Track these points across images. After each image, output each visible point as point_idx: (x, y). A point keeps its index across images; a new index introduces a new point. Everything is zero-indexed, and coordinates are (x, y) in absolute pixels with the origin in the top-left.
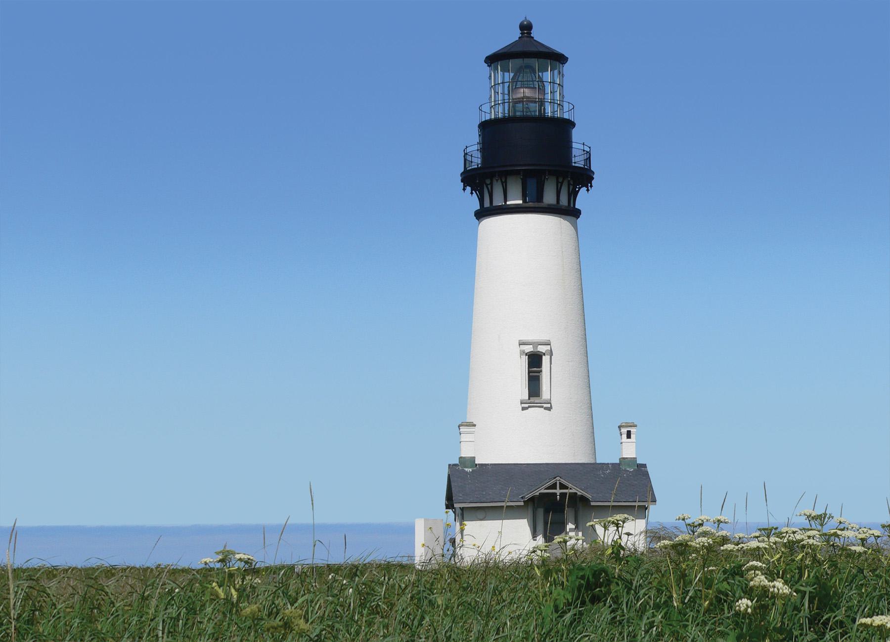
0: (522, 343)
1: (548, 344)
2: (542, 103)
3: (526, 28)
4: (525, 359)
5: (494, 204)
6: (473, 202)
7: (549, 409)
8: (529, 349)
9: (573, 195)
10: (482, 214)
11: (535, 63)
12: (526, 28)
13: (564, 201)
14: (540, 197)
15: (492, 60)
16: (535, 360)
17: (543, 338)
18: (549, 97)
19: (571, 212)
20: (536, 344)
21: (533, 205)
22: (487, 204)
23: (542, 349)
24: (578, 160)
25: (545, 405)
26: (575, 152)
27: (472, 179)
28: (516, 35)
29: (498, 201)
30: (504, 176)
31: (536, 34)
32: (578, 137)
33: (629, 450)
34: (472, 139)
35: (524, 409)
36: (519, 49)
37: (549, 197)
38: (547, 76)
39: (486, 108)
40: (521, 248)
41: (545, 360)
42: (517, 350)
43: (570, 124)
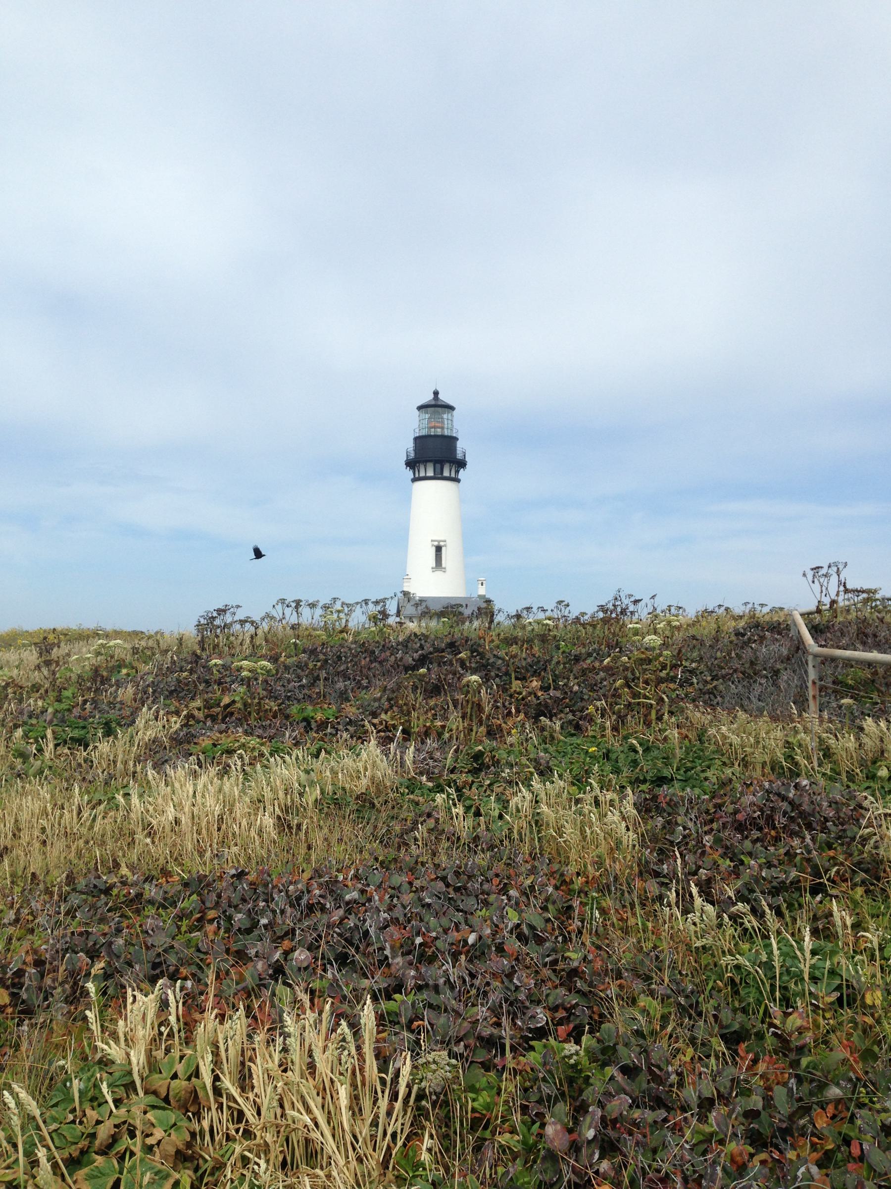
2: (443, 428)
3: (436, 393)
4: (434, 548)
6: (409, 474)
8: (436, 543)
9: (457, 472)
10: (414, 480)
11: (440, 409)
12: (436, 393)
14: (442, 473)
16: (439, 549)
17: (443, 539)
18: (446, 426)
20: (439, 541)
21: (438, 476)
22: (417, 475)
23: (442, 544)
24: (459, 456)
26: (458, 452)
27: (411, 464)
28: (432, 396)
29: (422, 474)
30: (425, 462)
31: (440, 396)
32: (460, 445)
33: (482, 591)
34: (410, 445)
36: (433, 403)
37: (446, 473)
38: (445, 416)
39: (417, 431)
40: (433, 497)
41: (443, 549)
42: (430, 544)
43: (456, 439)
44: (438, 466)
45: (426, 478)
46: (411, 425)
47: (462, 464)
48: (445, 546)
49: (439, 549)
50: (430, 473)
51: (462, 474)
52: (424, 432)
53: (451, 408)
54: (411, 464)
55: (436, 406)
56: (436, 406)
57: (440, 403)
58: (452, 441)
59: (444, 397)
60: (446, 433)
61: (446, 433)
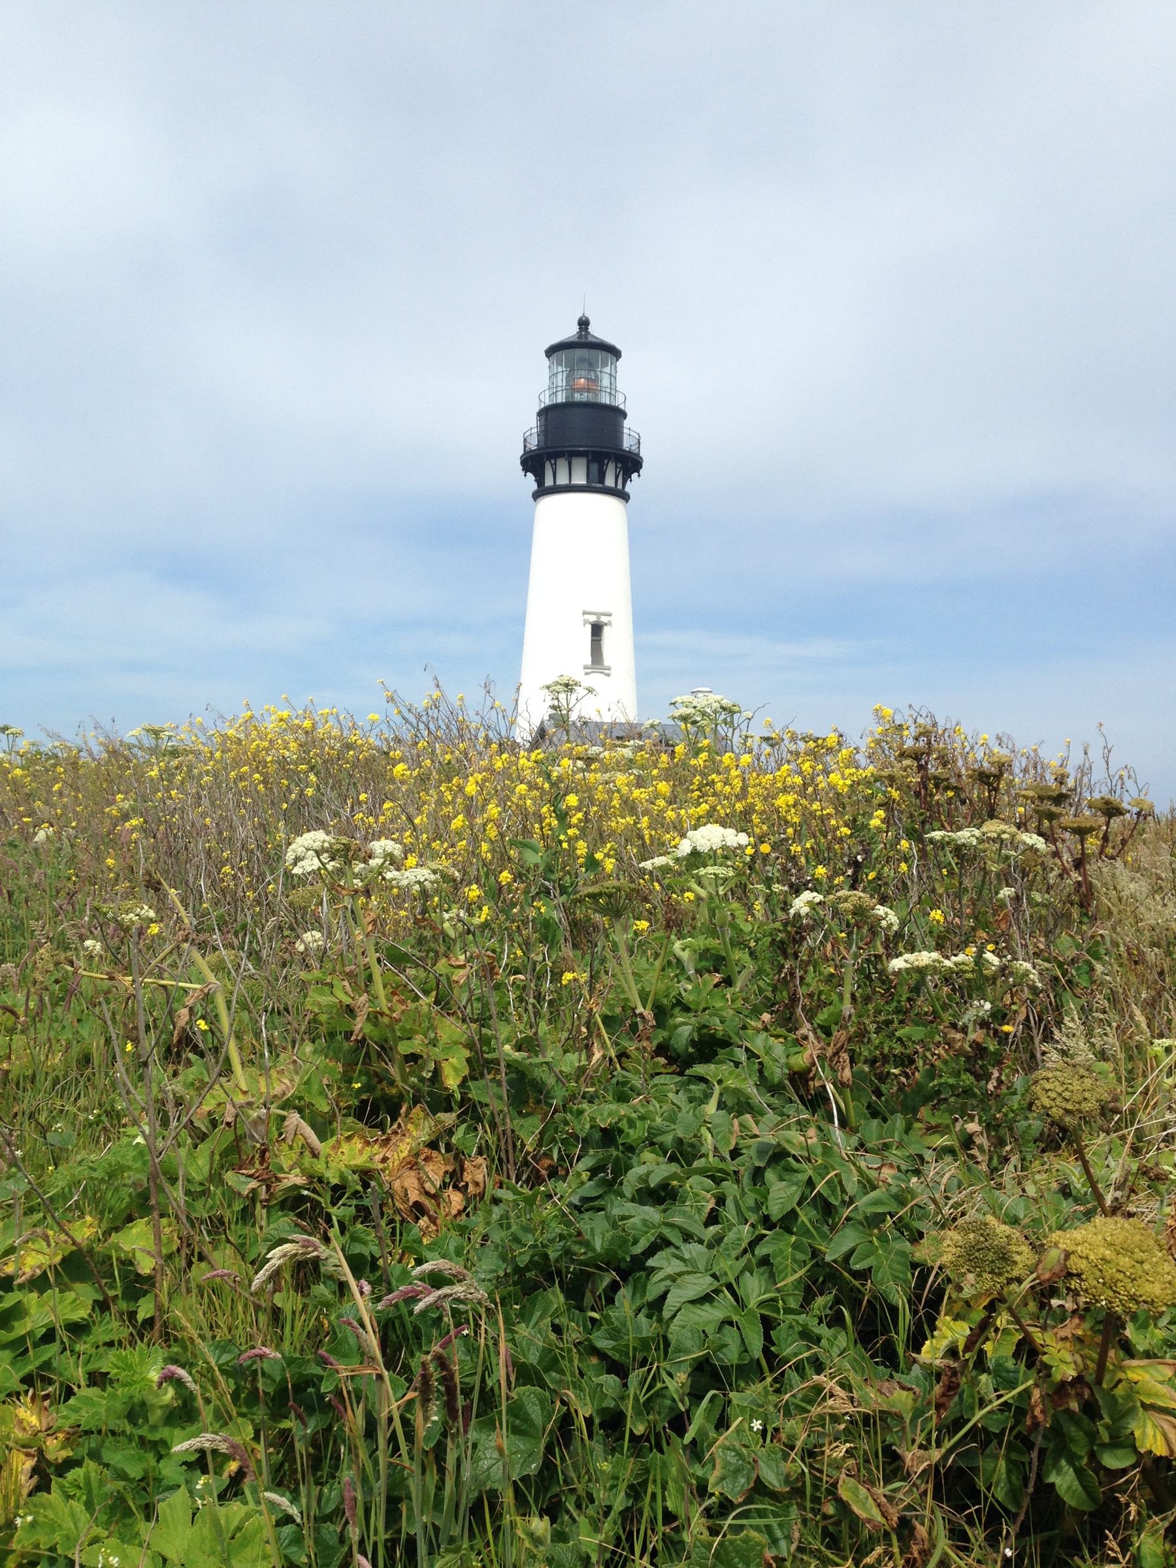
0: (585, 613)
1: (610, 615)
3: (584, 324)
4: (589, 627)
5: (559, 482)
6: (530, 481)
7: (608, 675)
8: (593, 618)
10: (542, 492)
12: (584, 324)
13: (620, 486)
14: (601, 479)
15: (551, 351)
16: (597, 630)
19: (624, 496)
20: (598, 614)
21: (595, 485)
22: (549, 482)
23: (604, 619)
29: (562, 480)
35: (586, 674)
37: (609, 482)
41: (606, 629)
42: (581, 618)
44: (595, 467)
46: (532, 387)
47: (631, 464)
49: (597, 630)
50: (580, 479)
51: (633, 486)
52: (561, 398)
53: (615, 353)
54: (533, 463)
55: (584, 350)
56: (584, 350)
57: (590, 339)
59: (597, 331)
60: (605, 399)
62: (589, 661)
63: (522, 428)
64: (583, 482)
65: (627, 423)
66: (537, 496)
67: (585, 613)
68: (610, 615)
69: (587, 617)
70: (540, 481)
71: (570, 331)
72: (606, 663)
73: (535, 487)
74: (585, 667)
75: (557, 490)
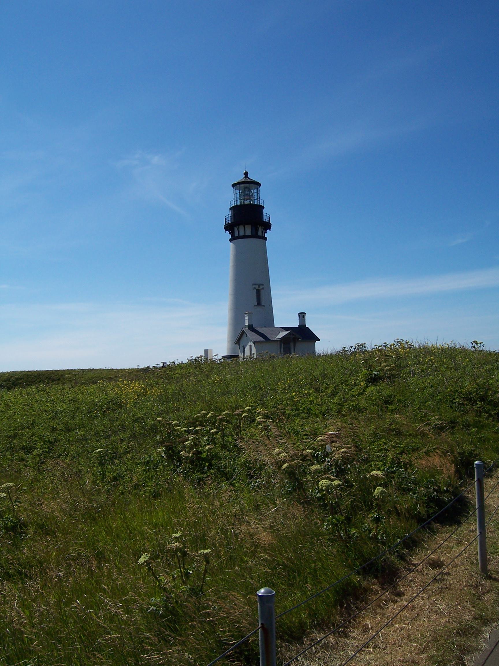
0: (254, 284)
1: (262, 285)
3: (246, 174)
8: (257, 287)
12: (246, 174)
15: (234, 185)
22: (236, 235)
25: (263, 307)
27: (229, 228)
29: (242, 233)
34: (227, 213)
37: (260, 233)
43: (263, 207)
45: (245, 237)
47: (267, 226)
48: (263, 289)
50: (249, 232)
51: (268, 234)
53: (259, 184)
54: (229, 228)
55: (247, 185)
56: (247, 185)
58: (260, 208)
61: (256, 203)
62: (256, 304)
63: (225, 214)
64: (250, 234)
65: (265, 211)
66: (231, 240)
67: (254, 284)
68: (262, 285)
69: (254, 286)
70: (233, 235)
71: (241, 178)
72: (263, 304)
73: (231, 237)
74: (255, 306)
75: (239, 237)
